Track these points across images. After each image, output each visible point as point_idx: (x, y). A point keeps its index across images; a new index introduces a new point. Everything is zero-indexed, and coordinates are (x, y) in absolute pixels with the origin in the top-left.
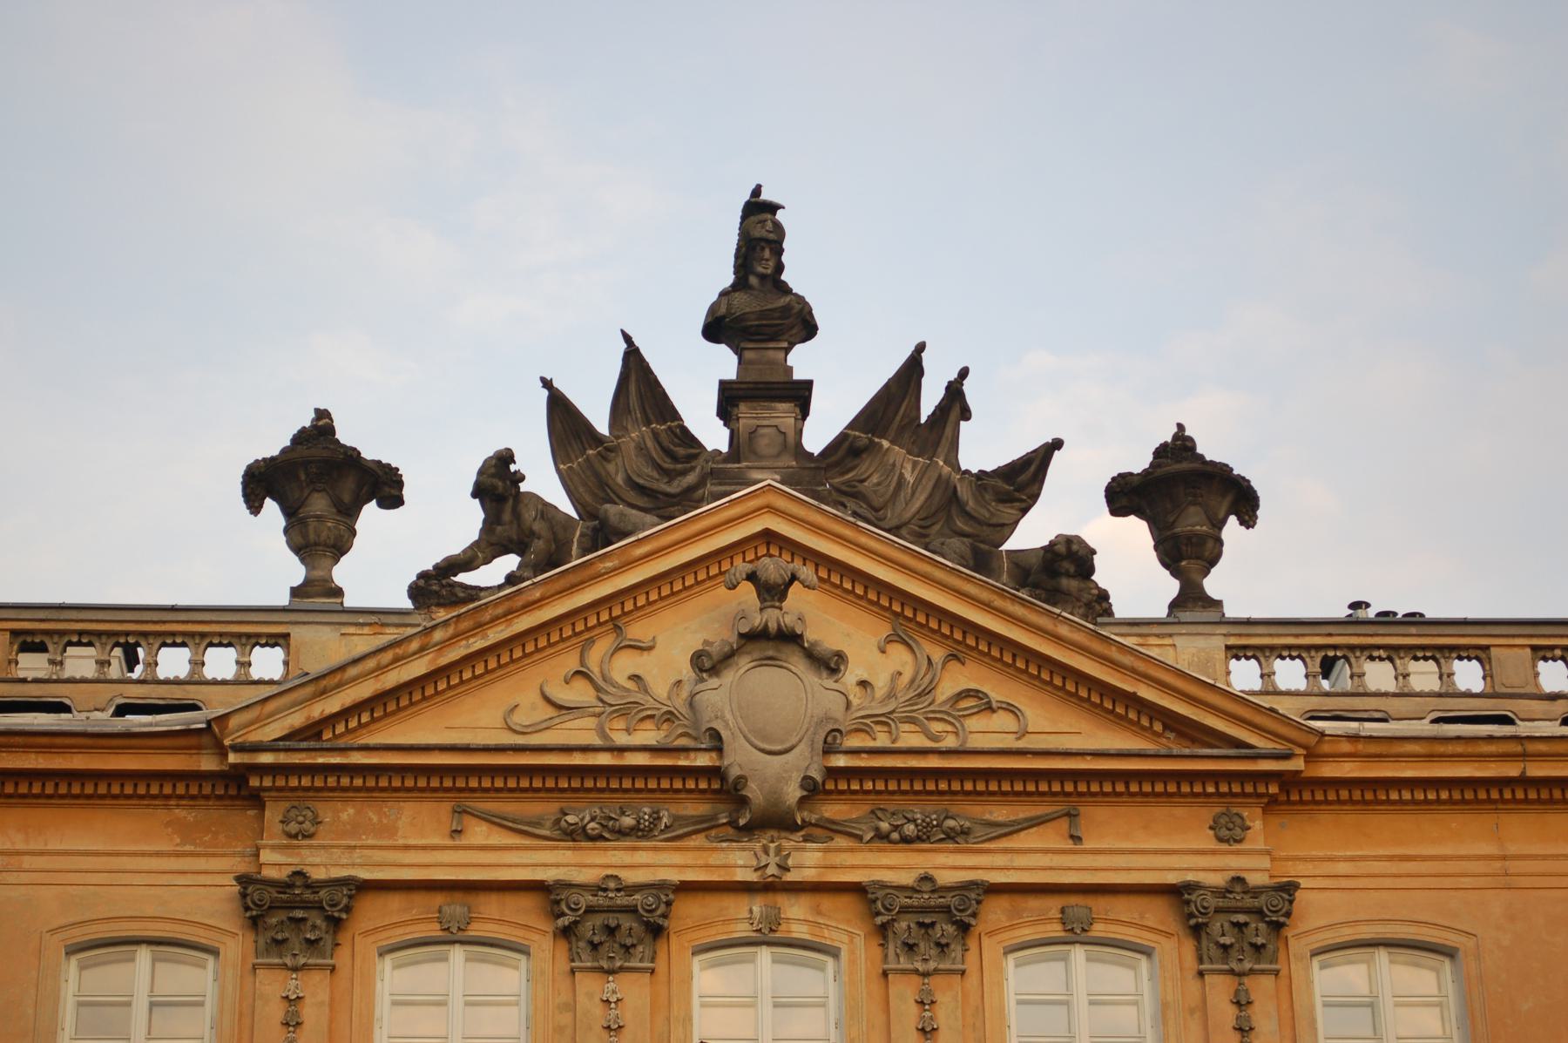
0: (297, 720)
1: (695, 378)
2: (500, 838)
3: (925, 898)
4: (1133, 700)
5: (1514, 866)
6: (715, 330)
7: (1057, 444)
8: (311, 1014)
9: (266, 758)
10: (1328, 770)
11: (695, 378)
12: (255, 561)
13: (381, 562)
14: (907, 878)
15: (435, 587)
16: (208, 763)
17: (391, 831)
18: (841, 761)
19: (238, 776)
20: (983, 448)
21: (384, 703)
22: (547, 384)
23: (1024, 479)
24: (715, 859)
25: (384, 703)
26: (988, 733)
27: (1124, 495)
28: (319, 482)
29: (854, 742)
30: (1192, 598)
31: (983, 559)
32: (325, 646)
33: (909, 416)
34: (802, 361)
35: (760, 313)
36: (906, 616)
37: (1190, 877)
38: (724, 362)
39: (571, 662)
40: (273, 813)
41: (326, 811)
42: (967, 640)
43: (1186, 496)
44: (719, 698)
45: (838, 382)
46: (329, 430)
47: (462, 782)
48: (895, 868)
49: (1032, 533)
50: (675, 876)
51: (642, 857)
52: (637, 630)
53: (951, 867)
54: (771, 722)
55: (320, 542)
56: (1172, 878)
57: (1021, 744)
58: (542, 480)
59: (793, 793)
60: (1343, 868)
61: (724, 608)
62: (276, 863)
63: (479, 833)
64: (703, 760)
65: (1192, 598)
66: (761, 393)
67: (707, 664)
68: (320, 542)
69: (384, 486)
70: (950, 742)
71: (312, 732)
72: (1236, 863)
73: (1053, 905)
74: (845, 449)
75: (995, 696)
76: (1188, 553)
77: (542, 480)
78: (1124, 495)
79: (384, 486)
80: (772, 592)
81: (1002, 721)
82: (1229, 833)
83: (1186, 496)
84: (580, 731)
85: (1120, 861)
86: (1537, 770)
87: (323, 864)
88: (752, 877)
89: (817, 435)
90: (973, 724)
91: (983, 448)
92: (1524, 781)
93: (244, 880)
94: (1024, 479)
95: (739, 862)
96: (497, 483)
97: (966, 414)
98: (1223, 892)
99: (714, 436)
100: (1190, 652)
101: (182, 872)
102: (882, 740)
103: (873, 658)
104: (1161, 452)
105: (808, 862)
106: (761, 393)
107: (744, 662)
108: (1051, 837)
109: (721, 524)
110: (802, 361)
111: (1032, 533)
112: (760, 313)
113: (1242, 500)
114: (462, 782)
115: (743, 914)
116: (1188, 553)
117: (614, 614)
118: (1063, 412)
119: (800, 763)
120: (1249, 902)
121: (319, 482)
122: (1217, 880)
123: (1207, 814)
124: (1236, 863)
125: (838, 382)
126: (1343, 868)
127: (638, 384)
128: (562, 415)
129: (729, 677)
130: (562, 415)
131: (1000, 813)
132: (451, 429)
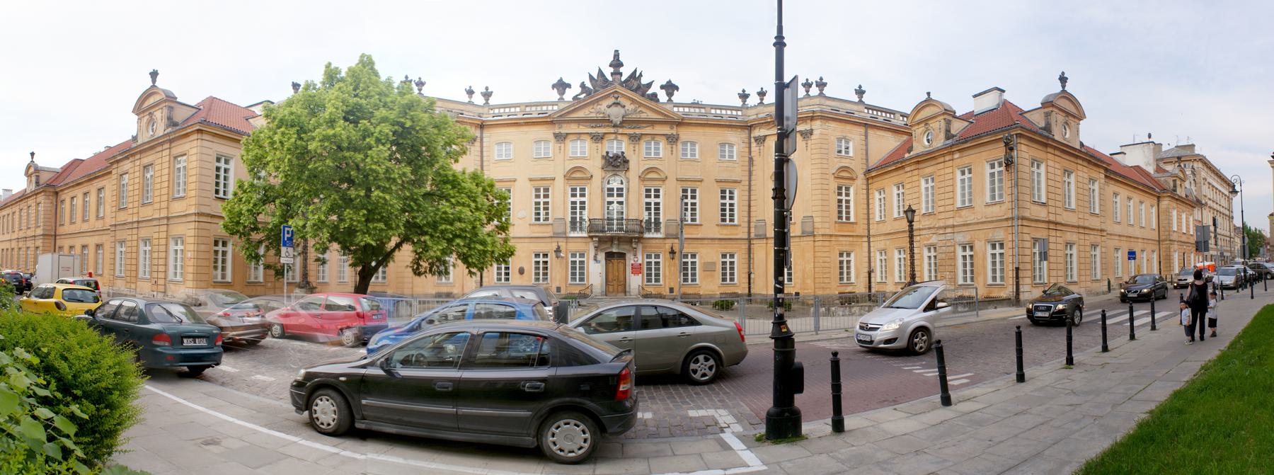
1: (608, 72)
11: (608, 72)
12: (555, 96)
13: (569, 95)
15: (575, 98)
20: (644, 81)
21: (569, 113)
23: (649, 85)
25: (569, 113)
26: (644, 116)
27: (662, 87)
28: (561, 86)
30: (670, 100)
31: (643, 95)
32: (562, 106)
33: (634, 76)
34: (621, 70)
35: (617, 64)
36: (633, 101)
38: (612, 70)
42: (641, 105)
43: (670, 88)
44: (608, 111)
45: (626, 72)
47: (579, 121)
48: (631, 131)
49: (650, 92)
53: (638, 131)
54: (616, 114)
55: (562, 93)
58: (588, 84)
61: (611, 101)
65: (670, 100)
66: (617, 73)
67: (609, 107)
68: (562, 93)
69: (569, 86)
74: (626, 81)
76: (670, 95)
77: (588, 84)
78: (662, 87)
79: (569, 86)
83: (670, 88)
87: (563, 131)
89: (623, 79)
91: (644, 81)
94: (649, 85)
95: (612, 130)
96: (583, 85)
99: (610, 78)
100: (669, 107)
101: (546, 133)
103: (630, 106)
105: (620, 131)
106: (617, 73)
109: (610, 90)
110: (621, 70)
111: (650, 92)
112: (617, 64)
114: (579, 121)
115: (613, 136)
116: (670, 95)
117: (597, 101)
118: (654, 77)
121: (561, 86)
125: (626, 72)
127: (601, 73)
128: (591, 77)
130: (591, 77)
132: (577, 79)
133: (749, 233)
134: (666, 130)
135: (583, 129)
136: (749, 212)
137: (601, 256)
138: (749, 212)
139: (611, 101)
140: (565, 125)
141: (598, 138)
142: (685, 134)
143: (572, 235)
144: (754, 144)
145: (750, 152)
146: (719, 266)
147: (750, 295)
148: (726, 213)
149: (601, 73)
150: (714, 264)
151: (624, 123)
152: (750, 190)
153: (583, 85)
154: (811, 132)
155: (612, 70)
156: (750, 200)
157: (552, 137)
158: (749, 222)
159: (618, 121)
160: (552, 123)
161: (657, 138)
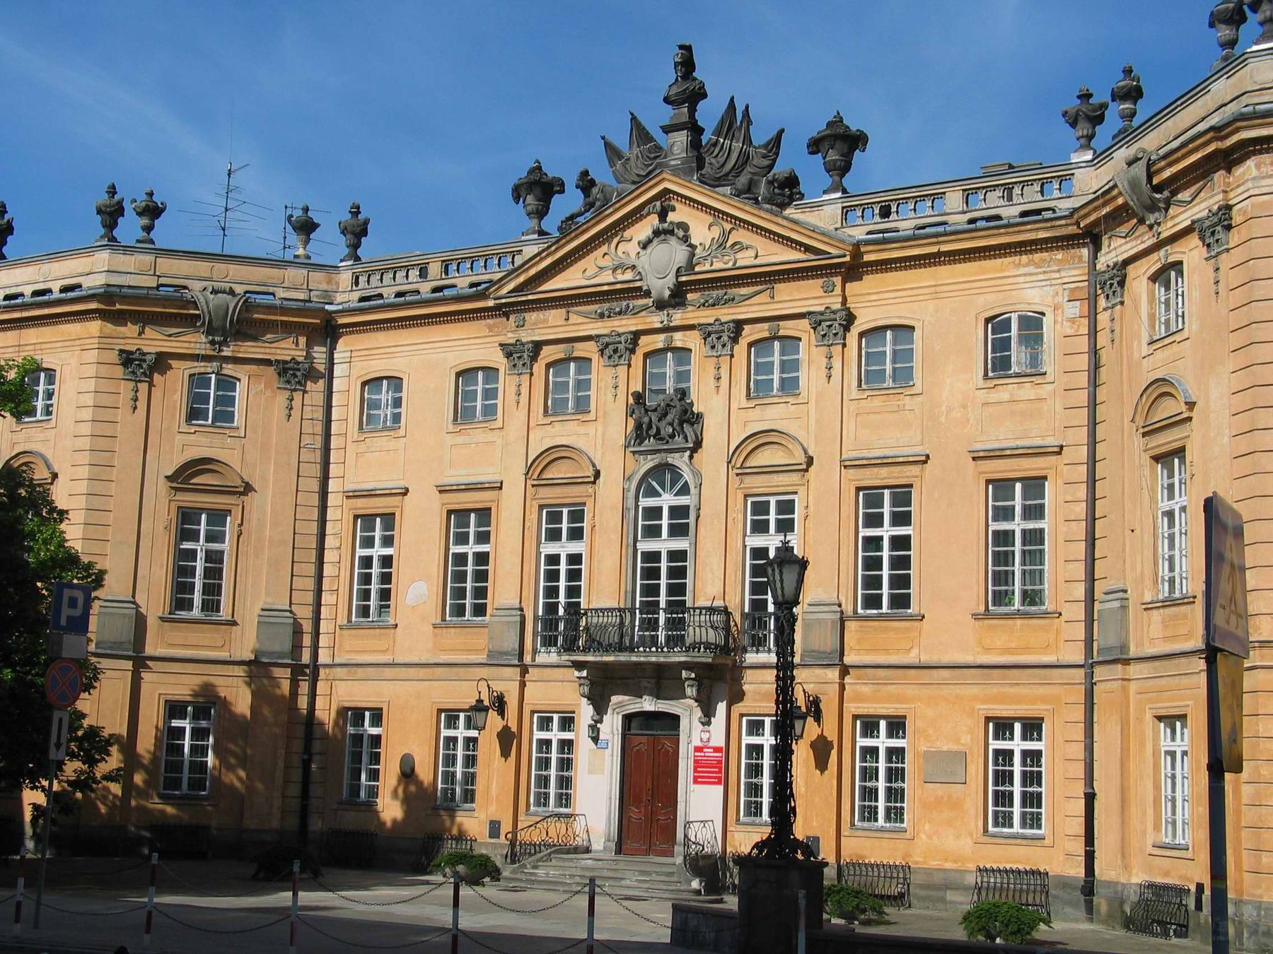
0: (511, 286)
2: (581, 320)
3: (715, 328)
4: (788, 239)
5: (939, 289)
6: (667, 100)
7: (783, 131)
8: (525, 391)
9: (503, 301)
10: (867, 258)
14: (711, 320)
16: (491, 303)
17: (546, 321)
18: (684, 279)
19: (498, 308)
20: (760, 136)
22: (603, 138)
24: (649, 320)
26: (745, 258)
27: (815, 146)
29: (697, 269)
37: (812, 309)
39: (604, 249)
40: (512, 318)
41: (527, 315)
46: (540, 168)
50: (634, 329)
51: (624, 322)
52: (627, 234)
53: (727, 314)
56: (804, 310)
57: (757, 262)
59: (667, 293)
60: (874, 297)
62: (510, 338)
63: (574, 318)
64: (638, 284)
67: (645, 245)
70: (730, 265)
71: (518, 289)
72: (828, 300)
73: (766, 326)
75: (746, 242)
76: (843, 168)
80: (663, 215)
81: (751, 253)
82: (828, 290)
84: (607, 277)
85: (787, 305)
86: (944, 248)
87: (527, 336)
88: (660, 326)
90: (739, 255)
91: (760, 136)
92: (939, 254)
93: (501, 345)
95: (656, 320)
96: (586, 183)
97: (750, 122)
98: (822, 314)
102: (707, 267)
103: (702, 232)
104: (830, 124)
105: (678, 317)
107: (655, 241)
108: (763, 298)
113: (856, 141)
119: (670, 280)
120: (832, 316)
122: (822, 309)
123: (820, 281)
124: (828, 300)
126: (874, 297)
129: (649, 249)
130: (612, 152)
131: (744, 291)
133: (1089, 641)
134: (808, 296)
135: (581, 323)
136: (1091, 560)
137: (612, 725)
138: (1091, 560)
139: (643, 230)
140: (532, 317)
141: (618, 349)
142: (875, 301)
143: (542, 658)
144: (1102, 302)
145: (1093, 332)
146: (977, 772)
147: (1088, 887)
148: (1011, 575)
149: (639, 133)
150: (962, 757)
151: (678, 297)
152: (1092, 481)
153: (586, 183)
154: (1223, 218)
155: (667, 114)
156: (1092, 519)
157: (498, 359)
158: (1090, 599)
159: (662, 286)
160: (503, 311)
161: (787, 328)
